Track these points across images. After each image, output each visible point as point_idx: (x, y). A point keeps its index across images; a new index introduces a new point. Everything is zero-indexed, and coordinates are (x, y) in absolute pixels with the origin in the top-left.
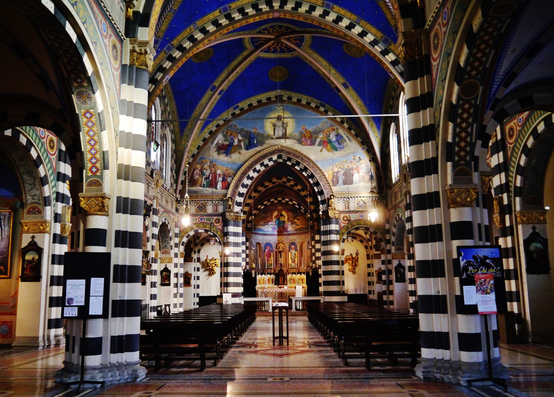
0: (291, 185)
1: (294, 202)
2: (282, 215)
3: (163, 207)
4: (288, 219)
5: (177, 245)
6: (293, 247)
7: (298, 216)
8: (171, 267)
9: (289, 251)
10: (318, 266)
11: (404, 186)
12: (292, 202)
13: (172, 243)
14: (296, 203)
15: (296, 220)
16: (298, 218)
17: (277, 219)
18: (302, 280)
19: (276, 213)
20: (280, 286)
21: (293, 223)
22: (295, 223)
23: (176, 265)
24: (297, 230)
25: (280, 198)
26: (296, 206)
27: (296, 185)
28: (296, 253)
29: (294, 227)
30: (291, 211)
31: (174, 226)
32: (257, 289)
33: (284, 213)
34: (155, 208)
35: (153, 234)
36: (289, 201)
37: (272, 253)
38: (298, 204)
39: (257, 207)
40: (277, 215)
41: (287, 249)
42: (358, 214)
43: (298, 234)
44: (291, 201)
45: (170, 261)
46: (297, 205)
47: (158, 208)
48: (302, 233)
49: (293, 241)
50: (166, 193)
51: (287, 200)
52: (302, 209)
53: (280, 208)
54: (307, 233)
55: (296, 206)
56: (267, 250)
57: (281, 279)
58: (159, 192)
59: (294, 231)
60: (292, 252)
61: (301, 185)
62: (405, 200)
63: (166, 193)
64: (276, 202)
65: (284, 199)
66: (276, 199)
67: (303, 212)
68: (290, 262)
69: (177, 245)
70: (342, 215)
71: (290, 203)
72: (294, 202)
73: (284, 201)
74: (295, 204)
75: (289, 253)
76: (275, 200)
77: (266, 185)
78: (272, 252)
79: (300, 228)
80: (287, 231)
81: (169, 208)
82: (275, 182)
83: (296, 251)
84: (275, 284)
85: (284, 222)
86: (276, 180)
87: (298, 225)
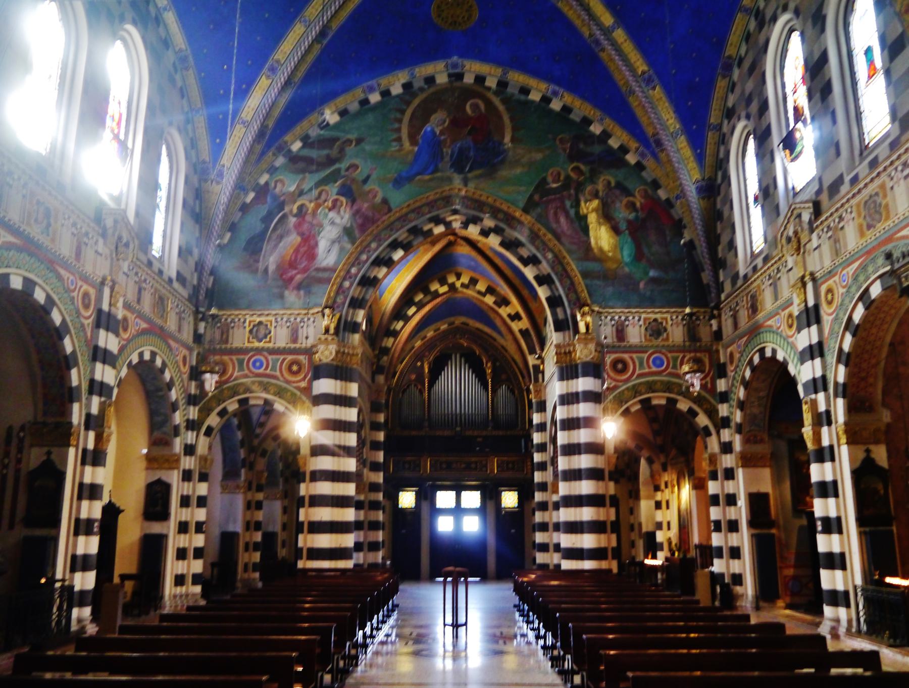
3: (141, 316)
5: (192, 425)
8: (174, 478)
11: (790, 265)
13: (178, 418)
23: (187, 476)
31: (185, 377)
34: (105, 307)
35: (92, 382)
42: (646, 356)
45: (172, 462)
47: (120, 313)
50: (158, 286)
58: (132, 274)
62: (796, 301)
63: (158, 286)
69: (192, 425)
70: (609, 359)
81: (171, 324)
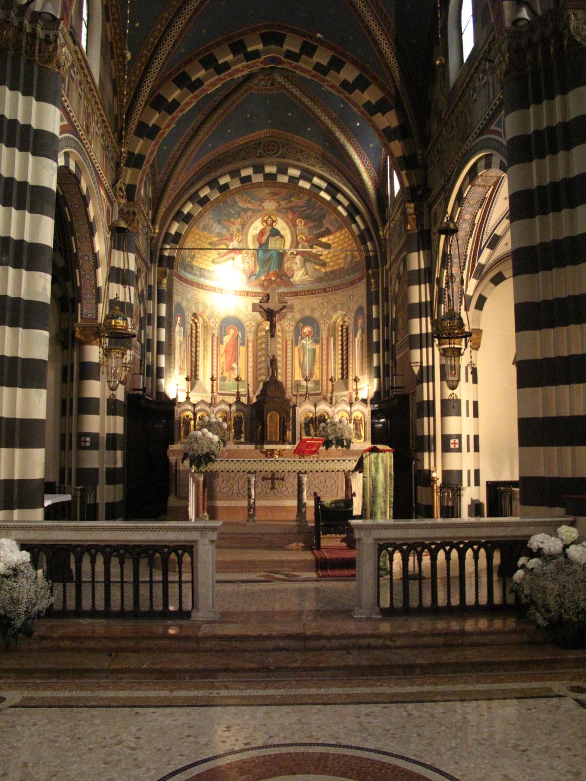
0: (318, 67)
1: (316, 180)
2: (275, 233)
4: (295, 243)
6: (307, 330)
7: (328, 232)
9: (296, 342)
10: (416, 370)
12: (309, 180)
14: (324, 185)
15: (317, 250)
16: (324, 240)
17: (261, 245)
18: (357, 423)
19: (257, 227)
20: (267, 447)
21: (308, 258)
22: (316, 256)
24: (319, 280)
25: (272, 164)
26: (323, 194)
27: (336, 64)
28: (317, 347)
29: (310, 271)
30: (307, 218)
32: (172, 459)
33: (281, 225)
36: (302, 177)
37: (242, 349)
38: (333, 189)
39: (196, 193)
40: (262, 233)
41: (290, 336)
43: (325, 290)
44: (307, 175)
46: (326, 191)
48: (338, 288)
49: (307, 313)
51: (294, 172)
52: (340, 203)
53: (270, 205)
54: (352, 283)
55: (323, 194)
56: (227, 339)
57: (272, 419)
59: (313, 282)
60: (303, 347)
61: (355, 63)
64: (258, 178)
65: (283, 171)
66: (259, 169)
67: (345, 214)
68: (298, 377)
71: (304, 184)
72: (316, 180)
73: (283, 179)
74: (321, 189)
75: (296, 349)
76: (255, 172)
77: (221, 62)
78: (243, 344)
79: (332, 272)
80: (291, 285)
82: (256, 54)
83: (316, 342)
84: (249, 441)
85: (281, 255)
86: (260, 47)
87: (324, 264)
